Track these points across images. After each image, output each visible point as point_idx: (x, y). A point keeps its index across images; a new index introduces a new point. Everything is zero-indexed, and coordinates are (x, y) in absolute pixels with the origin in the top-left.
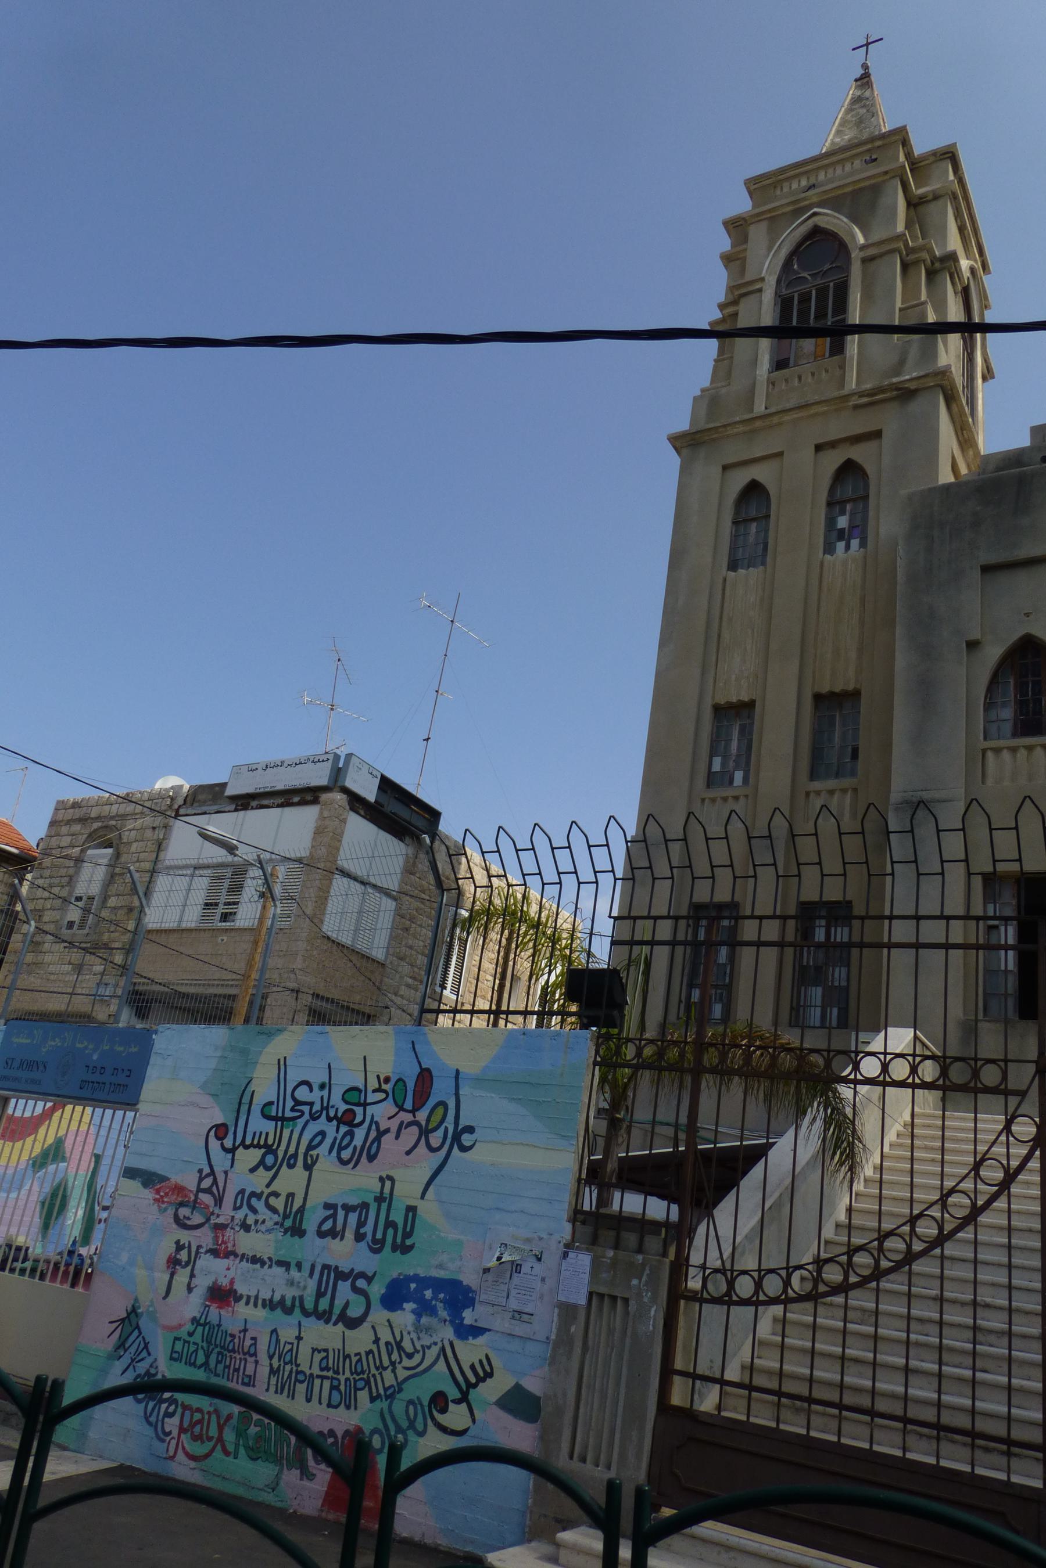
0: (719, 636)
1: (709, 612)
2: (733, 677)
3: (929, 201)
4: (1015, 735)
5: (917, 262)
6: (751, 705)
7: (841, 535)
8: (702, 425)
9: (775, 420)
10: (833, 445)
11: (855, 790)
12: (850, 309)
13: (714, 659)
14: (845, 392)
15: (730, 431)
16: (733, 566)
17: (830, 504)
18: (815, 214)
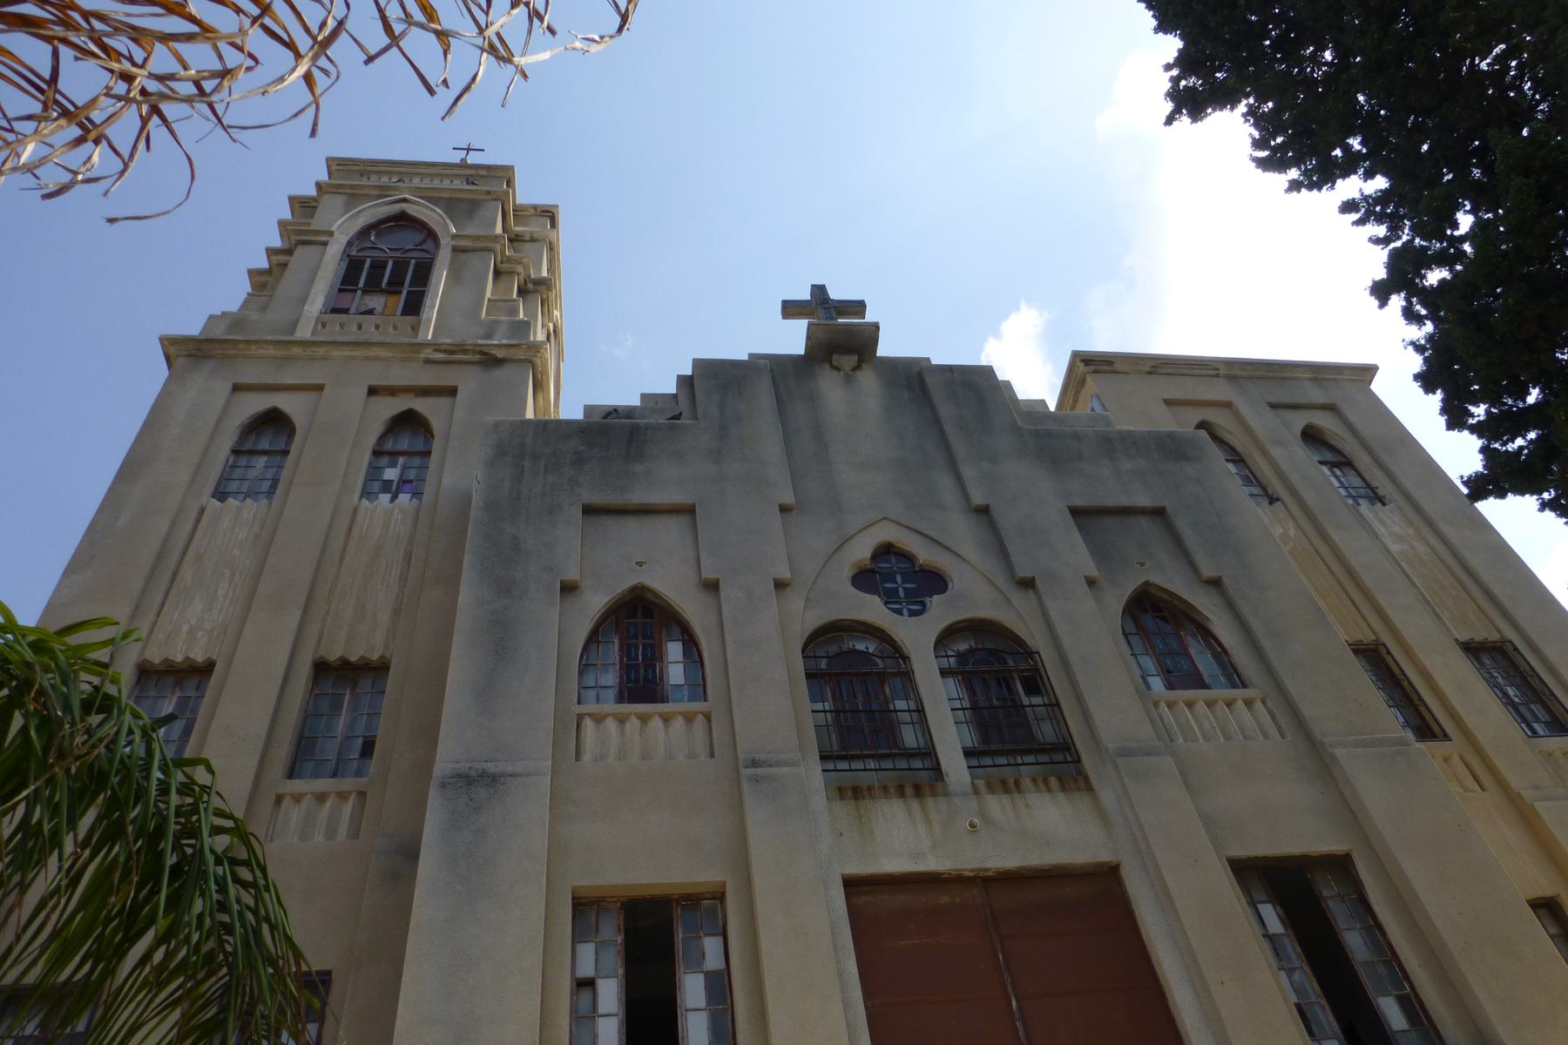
0: (175, 574)
1: (166, 540)
2: (185, 628)
4: (620, 699)
5: (511, 273)
6: (205, 670)
7: (386, 486)
8: (218, 333)
9: (321, 351)
10: (392, 391)
11: (362, 795)
12: (433, 280)
13: (158, 599)
14: (420, 339)
15: (254, 350)
16: (221, 495)
17: (377, 453)
18: (405, 200)
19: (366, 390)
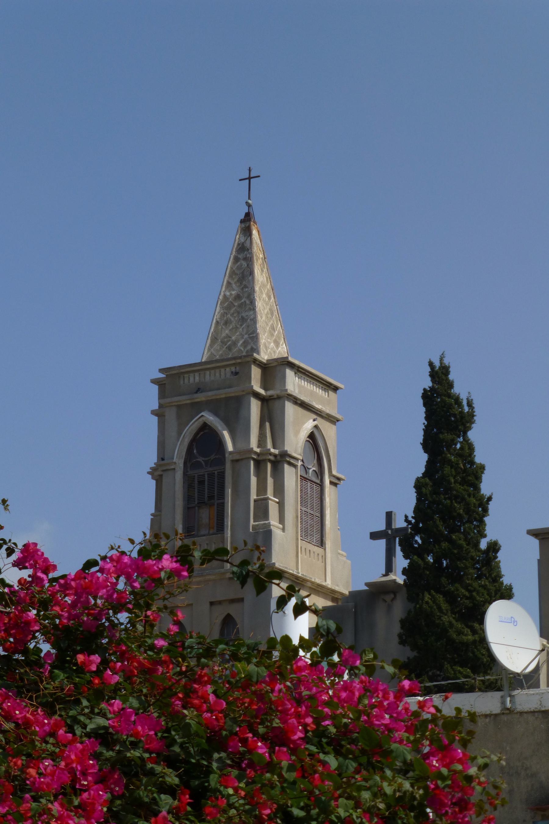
5: (265, 461)
18: (202, 416)
19: (208, 604)
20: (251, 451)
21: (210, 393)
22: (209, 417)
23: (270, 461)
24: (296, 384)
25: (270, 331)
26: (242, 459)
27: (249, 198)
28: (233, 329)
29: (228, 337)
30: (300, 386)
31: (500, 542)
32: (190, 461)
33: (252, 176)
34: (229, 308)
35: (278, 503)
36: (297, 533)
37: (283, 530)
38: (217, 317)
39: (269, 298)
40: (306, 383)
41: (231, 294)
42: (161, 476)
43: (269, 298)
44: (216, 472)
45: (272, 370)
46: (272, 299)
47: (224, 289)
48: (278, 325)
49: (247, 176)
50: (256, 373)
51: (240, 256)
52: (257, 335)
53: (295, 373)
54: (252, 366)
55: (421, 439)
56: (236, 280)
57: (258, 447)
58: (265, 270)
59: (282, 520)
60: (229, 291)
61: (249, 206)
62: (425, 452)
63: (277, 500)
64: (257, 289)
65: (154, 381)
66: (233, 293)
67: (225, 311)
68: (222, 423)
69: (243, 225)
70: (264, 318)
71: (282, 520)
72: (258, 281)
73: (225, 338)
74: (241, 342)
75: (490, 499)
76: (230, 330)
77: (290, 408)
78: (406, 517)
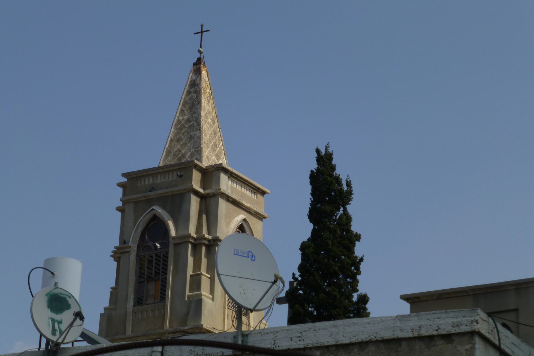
3: (211, 196)
5: (201, 245)
18: (153, 209)
20: (189, 236)
21: (160, 192)
22: (159, 210)
23: (204, 244)
24: (229, 186)
25: (212, 147)
26: (182, 243)
27: (201, 47)
28: (183, 144)
29: (179, 150)
30: (232, 188)
31: (369, 295)
32: (142, 245)
33: (204, 30)
34: (181, 129)
35: (210, 278)
36: (225, 303)
37: (213, 299)
38: (172, 135)
39: (214, 123)
40: (238, 186)
41: (183, 119)
42: (120, 258)
43: (214, 123)
44: (162, 254)
45: (210, 174)
46: (216, 123)
47: (178, 115)
48: (219, 143)
49: (200, 31)
50: (196, 176)
51: (191, 90)
52: (201, 148)
53: (229, 178)
54: (194, 170)
55: (307, 211)
56: (187, 108)
57: (196, 234)
58: (211, 101)
59: (212, 292)
60: (182, 116)
61: (200, 52)
62: (311, 222)
63: (209, 276)
64: (203, 114)
65: (119, 185)
66: (185, 117)
67: (178, 131)
68: (168, 215)
69: (195, 67)
70: (208, 137)
71: (212, 292)
72: (204, 109)
73: (176, 151)
74: (189, 154)
75: (362, 260)
76: (181, 146)
77: (222, 204)
78: (294, 275)
